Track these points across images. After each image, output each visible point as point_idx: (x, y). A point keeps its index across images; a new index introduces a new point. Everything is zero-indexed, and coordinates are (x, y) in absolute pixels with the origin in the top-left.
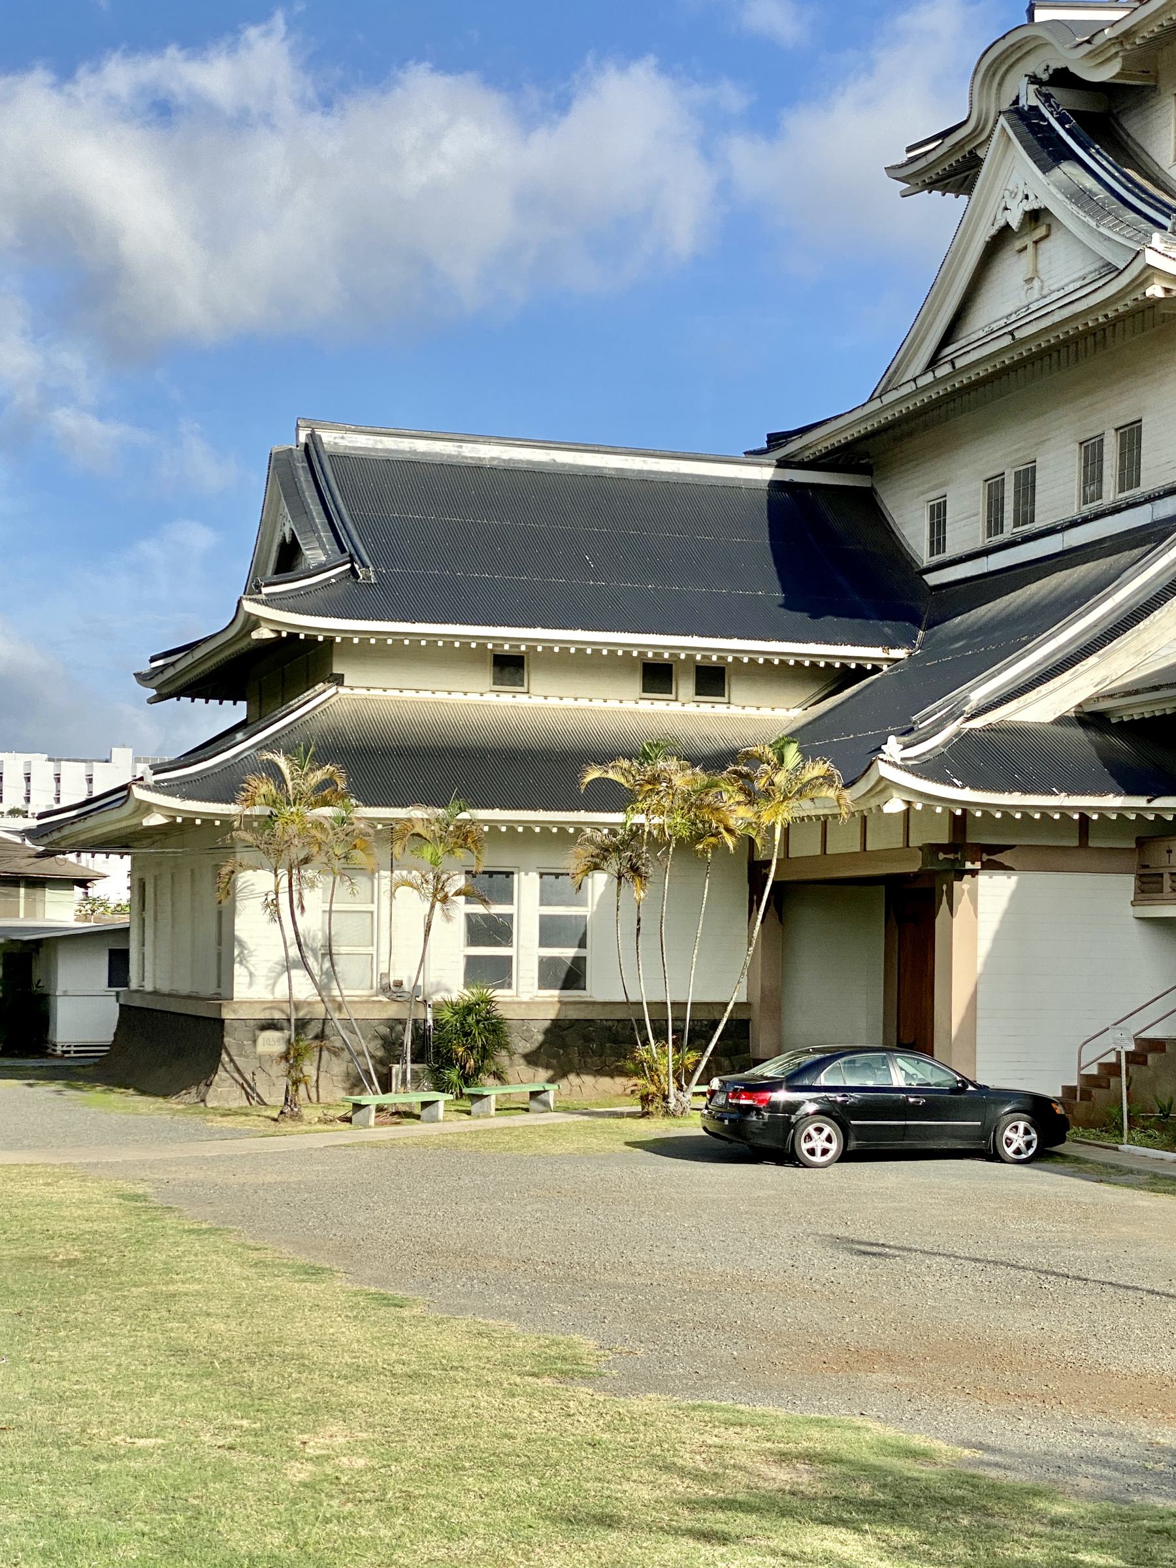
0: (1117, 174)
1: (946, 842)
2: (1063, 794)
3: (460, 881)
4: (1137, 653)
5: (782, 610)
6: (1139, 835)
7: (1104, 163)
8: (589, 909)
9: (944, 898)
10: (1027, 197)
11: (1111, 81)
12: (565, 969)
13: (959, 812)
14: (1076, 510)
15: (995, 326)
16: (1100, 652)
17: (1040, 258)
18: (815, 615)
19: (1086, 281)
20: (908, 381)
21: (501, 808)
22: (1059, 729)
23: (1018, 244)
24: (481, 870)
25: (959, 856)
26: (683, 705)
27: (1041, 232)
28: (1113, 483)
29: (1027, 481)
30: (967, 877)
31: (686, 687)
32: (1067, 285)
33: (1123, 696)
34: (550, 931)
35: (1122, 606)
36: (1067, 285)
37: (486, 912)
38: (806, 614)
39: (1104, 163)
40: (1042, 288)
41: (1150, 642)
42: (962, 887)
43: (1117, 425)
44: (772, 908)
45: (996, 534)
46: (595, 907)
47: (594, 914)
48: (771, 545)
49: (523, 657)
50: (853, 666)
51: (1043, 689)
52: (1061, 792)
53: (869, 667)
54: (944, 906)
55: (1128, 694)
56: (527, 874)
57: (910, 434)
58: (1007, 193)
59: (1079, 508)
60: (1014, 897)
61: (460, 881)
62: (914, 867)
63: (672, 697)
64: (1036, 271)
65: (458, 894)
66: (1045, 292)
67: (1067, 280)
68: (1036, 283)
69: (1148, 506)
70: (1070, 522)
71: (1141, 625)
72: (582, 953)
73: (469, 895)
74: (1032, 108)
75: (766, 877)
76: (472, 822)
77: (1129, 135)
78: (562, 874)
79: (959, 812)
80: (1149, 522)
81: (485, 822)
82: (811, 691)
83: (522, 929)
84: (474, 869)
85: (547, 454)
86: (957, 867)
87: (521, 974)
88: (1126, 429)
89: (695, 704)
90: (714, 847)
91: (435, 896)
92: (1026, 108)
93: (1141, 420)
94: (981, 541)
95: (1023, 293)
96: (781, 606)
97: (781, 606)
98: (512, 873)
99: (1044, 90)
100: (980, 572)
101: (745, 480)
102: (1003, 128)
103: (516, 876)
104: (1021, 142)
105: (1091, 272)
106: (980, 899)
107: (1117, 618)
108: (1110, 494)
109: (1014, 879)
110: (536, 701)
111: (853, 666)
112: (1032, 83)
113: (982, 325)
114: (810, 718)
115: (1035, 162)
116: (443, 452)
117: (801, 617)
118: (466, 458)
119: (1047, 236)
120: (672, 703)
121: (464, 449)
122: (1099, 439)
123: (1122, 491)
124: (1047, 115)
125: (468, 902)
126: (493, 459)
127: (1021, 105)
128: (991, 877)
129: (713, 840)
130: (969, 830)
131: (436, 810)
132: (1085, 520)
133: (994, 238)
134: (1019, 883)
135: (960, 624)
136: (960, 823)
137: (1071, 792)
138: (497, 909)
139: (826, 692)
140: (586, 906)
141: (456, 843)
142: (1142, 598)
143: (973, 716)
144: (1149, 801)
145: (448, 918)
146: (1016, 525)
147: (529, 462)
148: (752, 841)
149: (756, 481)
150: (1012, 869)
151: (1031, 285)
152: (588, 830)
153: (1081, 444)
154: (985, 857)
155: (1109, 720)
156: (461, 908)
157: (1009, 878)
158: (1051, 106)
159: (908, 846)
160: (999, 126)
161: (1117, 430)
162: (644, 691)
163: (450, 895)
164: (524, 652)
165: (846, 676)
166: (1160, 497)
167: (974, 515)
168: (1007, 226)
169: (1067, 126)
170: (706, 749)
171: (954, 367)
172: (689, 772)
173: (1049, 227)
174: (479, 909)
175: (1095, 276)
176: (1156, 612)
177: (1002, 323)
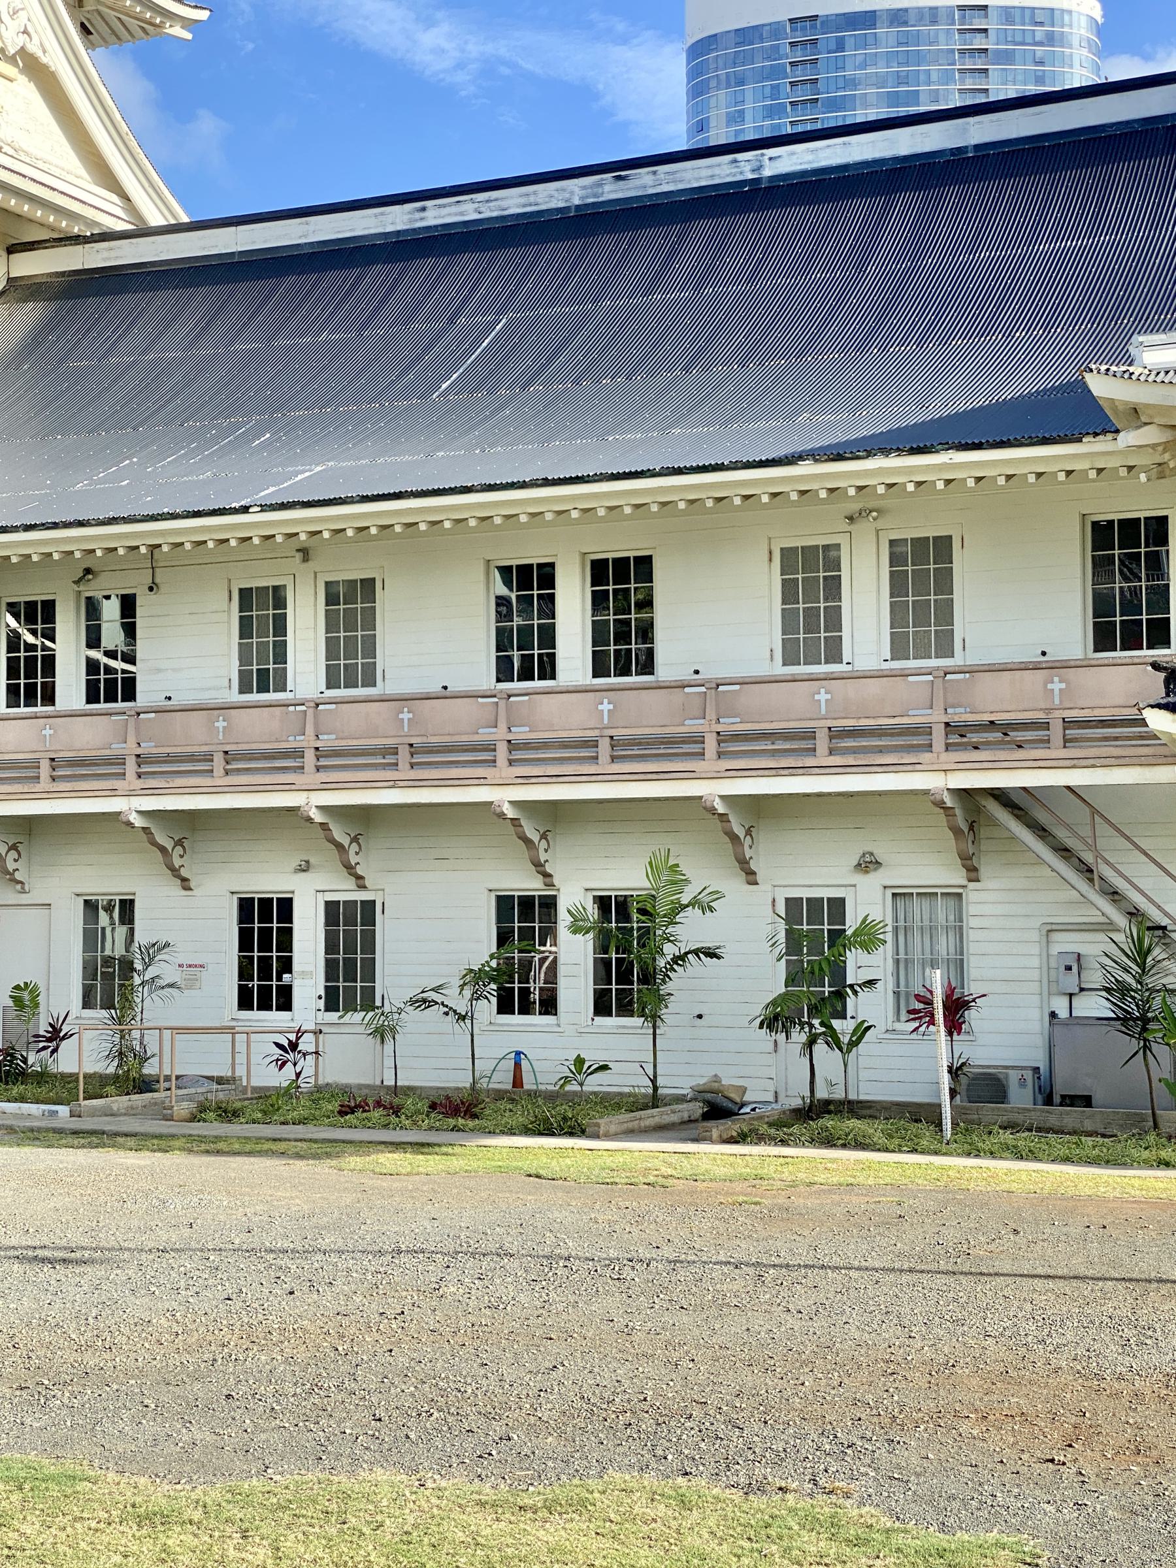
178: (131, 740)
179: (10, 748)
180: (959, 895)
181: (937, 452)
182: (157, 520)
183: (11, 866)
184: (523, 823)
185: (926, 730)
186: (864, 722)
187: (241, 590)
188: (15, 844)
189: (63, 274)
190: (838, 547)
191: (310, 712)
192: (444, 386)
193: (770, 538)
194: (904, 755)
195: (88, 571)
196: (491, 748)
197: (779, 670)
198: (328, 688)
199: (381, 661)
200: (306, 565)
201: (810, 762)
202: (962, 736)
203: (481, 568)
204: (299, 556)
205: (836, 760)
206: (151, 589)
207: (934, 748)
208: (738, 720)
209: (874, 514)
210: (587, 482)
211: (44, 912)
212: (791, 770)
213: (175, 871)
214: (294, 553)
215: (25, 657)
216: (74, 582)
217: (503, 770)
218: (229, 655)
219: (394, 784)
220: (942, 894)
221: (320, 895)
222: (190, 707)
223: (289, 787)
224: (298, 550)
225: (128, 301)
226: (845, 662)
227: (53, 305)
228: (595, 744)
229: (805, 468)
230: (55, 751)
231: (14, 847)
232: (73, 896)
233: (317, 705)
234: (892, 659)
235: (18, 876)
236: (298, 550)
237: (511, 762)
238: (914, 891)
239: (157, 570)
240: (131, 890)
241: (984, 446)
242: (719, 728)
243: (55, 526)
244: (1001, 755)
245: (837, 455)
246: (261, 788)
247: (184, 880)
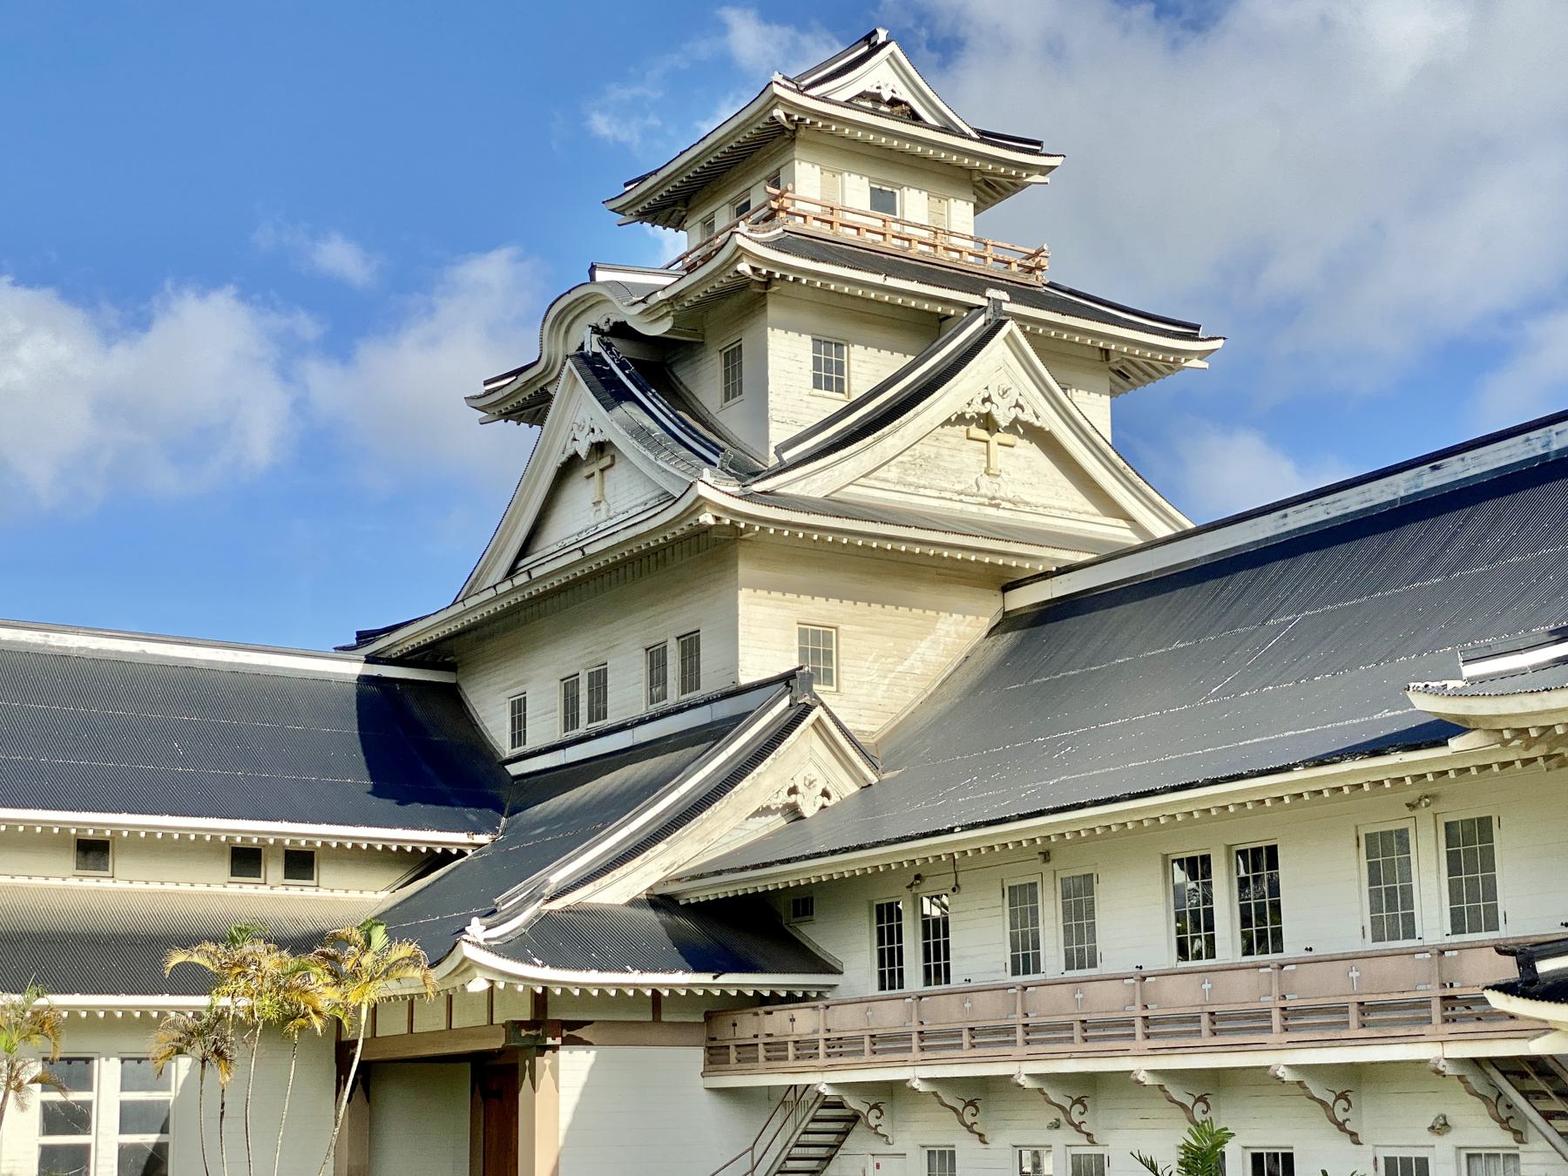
0: (671, 416)
1: (529, 1019)
2: (637, 971)
3: (37, 1069)
4: (701, 841)
5: (369, 796)
6: (706, 1009)
7: (660, 405)
8: (173, 1093)
9: (527, 1073)
10: (593, 431)
11: (667, 336)
12: (147, 1155)
13: (539, 990)
14: (644, 709)
15: (567, 542)
16: (668, 839)
17: (607, 485)
18: (402, 802)
19: (648, 506)
20: (489, 588)
21: (82, 993)
22: (632, 911)
24: (58, 1056)
25: (540, 1032)
26: (272, 888)
27: (606, 461)
28: (676, 686)
29: (599, 681)
30: (549, 1053)
31: (274, 870)
32: (631, 509)
33: (689, 880)
34: (131, 1118)
35: (686, 797)
36: (631, 509)
37: (63, 1099)
38: (394, 801)
39: (660, 405)
40: (608, 511)
41: (713, 830)
42: (544, 1062)
44: (359, 1086)
45: (572, 729)
46: (178, 1092)
47: (176, 1099)
48: (360, 735)
49: (107, 842)
50: (439, 850)
51: (618, 873)
52: (634, 970)
53: (454, 851)
54: (527, 1081)
55: (694, 878)
56: (107, 1060)
57: (491, 635)
58: (575, 426)
59: (647, 707)
60: (593, 1068)
61: (37, 1069)
62: (498, 1044)
63: (261, 880)
64: (602, 495)
65: (33, 1081)
66: (611, 514)
68: (603, 506)
69: (708, 706)
70: (639, 719)
71: (704, 815)
72: (164, 1138)
73: (45, 1082)
74: (595, 354)
75: (353, 1056)
76: (50, 1008)
77: (681, 383)
78: (143, 1059)
79: (539, 990)
80: (709, 721)
81: (65, 1008)
82: (398, 875)
83: (101, 1116)
84: (50, 1056)
85: (137, 645)
86: (540, 1043)
87: (99, 1163)
88: (687, 638)
89: (284, 888)
90: (302, 1028)
91: (8, 1084)
92: (590, 354)
93: (699, 631)
94: (558, 736)
95: (592, 514)
96: (369, 793)
97: (369, 793)
98: (92, 1059)
99: (605, 339)
100: (559, 764)
101: (334, 673)
102: (570, 370)
103: (96, 1062)
104: (586, 383)
105: (652, 499)
106: (562, 1074)
107: (682, 808)
108: (674, 696)
109: (593, 1053)
110: (122, 885)
111: (439, 850)
112: (595, 333)
113: (556, 540)
114: (398, 900)
115: (599, 401)
116: (29, 641)
117: (389, 804)
118: (53, 647)
119: (611, 466)
120: (260, 887)
121: (50, 639)
122: (662, 646)
123: (683, 693)
124: (609, 361)
125: (43, 1090)
126: (80, 648)
127: (586, 351)
128: (571, 1052)
129: (304, 1021)
130: (549, 1008)
131: (12, 996)
132: (652, 719)
134: (597, 1057)
135: (540, 812)
136: (541, 1001)
137: (643, 970)
138: (75, 1096)
139: (413, 875)
140: (169, 1089)
141: (31, 1030)
142: (704, 791)
143: (552, 899)
144: (715, 978)
145: (23, 1107)
146: (590, 721)
147: (118, 652)
148: (339, 1022)
149: (345, 674)
150: (591, 1044)
152: (173, 1014)
153: (647, 650)
154: (565, 1033)
155: (678, 902)
156: (37, 1096)
157: (588, 1052)
158: (612, 353)
159: (492, 1024)
160: (566, 367)
161: (678, 638)
162: (233, 875)
163: (25, 1082)
164: (108, 837)
165: (433, 860)
166: (717, 699)
167: (551, 712)
168: (576, 456)
169: (627, 372)
170: (293, 931)
171: (530, 577)
172: (277, 954)
173: (613, 457)
174: (56, 1096)
176: (717, 804)
177: (573, 540)
178: (915, 1022)
179: (849, 1027)
180: (1517, 1156)
181: (1389, 754)
182: (903, 842)
183: (873, 1122)
184: (1166, 1088)
185: (1424, 1004)
186: (1382, 997)
187: (1010, 887)
188: (876, 1104)
189: (1037, 604)
190: (1406, 830)
191: (1019, 993)
192: (1214, 690)
193: (1357, 827)
194: (1411, 1027)
195: (918, 877)
196: (1130, 1024)
197: (1370, 946)
198: (1066, 969)
199: (1102, 945)
200: (1046, 865)
201: (1345, 1034)
202: (1468, 1008)
203: (1159, 859)
204: (1042, 857)
205: (1364, 1033)
206: (954, 890)
207: (1434, 1021)
208: (1296, 997)
209: (1427, 800)
210: (1157, 794)
211: (896, 1161)
212: (1331, 1042)
213: (970, 1128)
214: (1038, 857)
215: (888, 948)
216: (908, 887)
217: (1141, 1044)
218: (1004, 943)
219: (1070, 1056)
220: (1504, 1155)
221: (1068, 1149)
222: (961, 990)
223: (1007, 1059)
224: (1040, 853)
225: (1071, 624)
226: (1417, 937)
227: (1021, 633)
228: (1196, 1019)
229: (1299, 774)
230: (872, 1029)
231: (876, 1106)
232: (919, 1148)
233: (1025, 988)
234: (1453, 934)
235: (880, 1130)
236: (1040, 853)
237: (1148, 1037)
238: (1483, 1152)
239: (959, 875)
240: (951, 1143)
241: (1423, 746)
242: (1283, 1004)
243: (847, 850)
244: (1471, 1027)
245: (1320, 762)
246: (990, 1059)
247: (981, 1135)
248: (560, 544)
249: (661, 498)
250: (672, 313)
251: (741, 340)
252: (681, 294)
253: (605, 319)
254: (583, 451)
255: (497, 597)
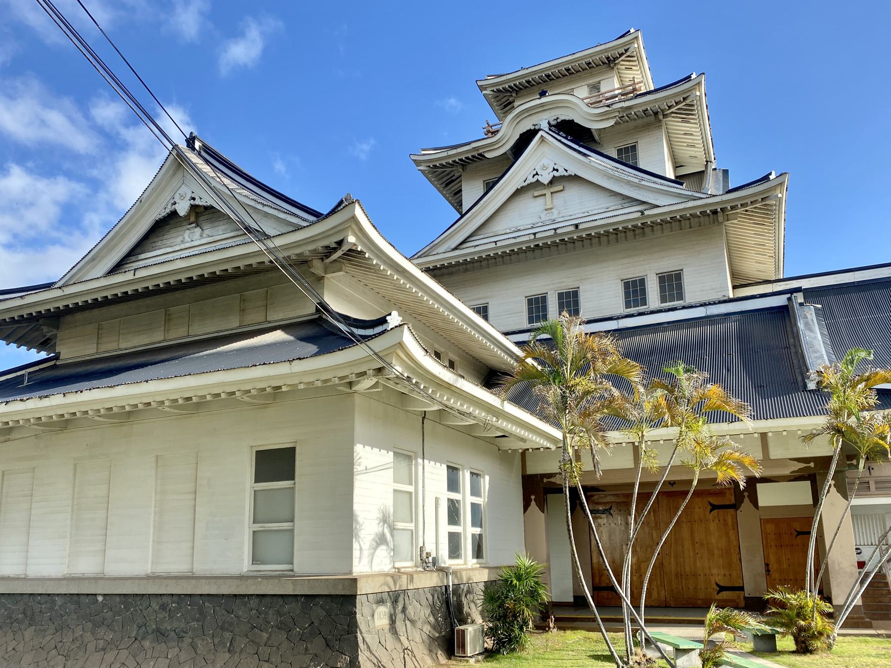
15: (522, 228)
17: (554, 201)
19: (608, 210)
23: (536, 194)
27: (561, 188)
32: (579, 213)
40: (559, 214)
43: (658, 272)
67: (579, 211)
69: (702, 308)
80: (704, 315)
88: (664, 274)
119: (562, 191)
133: (523, 187)
151: (549, 211)
166: (715, 303)
175: (620, 207)
177: (529, 226)
248: (514, 229)
249: (624, 205)
250: (617, 117)
251: (637, 142)
252: (634, 106)
253: (555, 117)
254: (545, 178)
255: (535, 240)
